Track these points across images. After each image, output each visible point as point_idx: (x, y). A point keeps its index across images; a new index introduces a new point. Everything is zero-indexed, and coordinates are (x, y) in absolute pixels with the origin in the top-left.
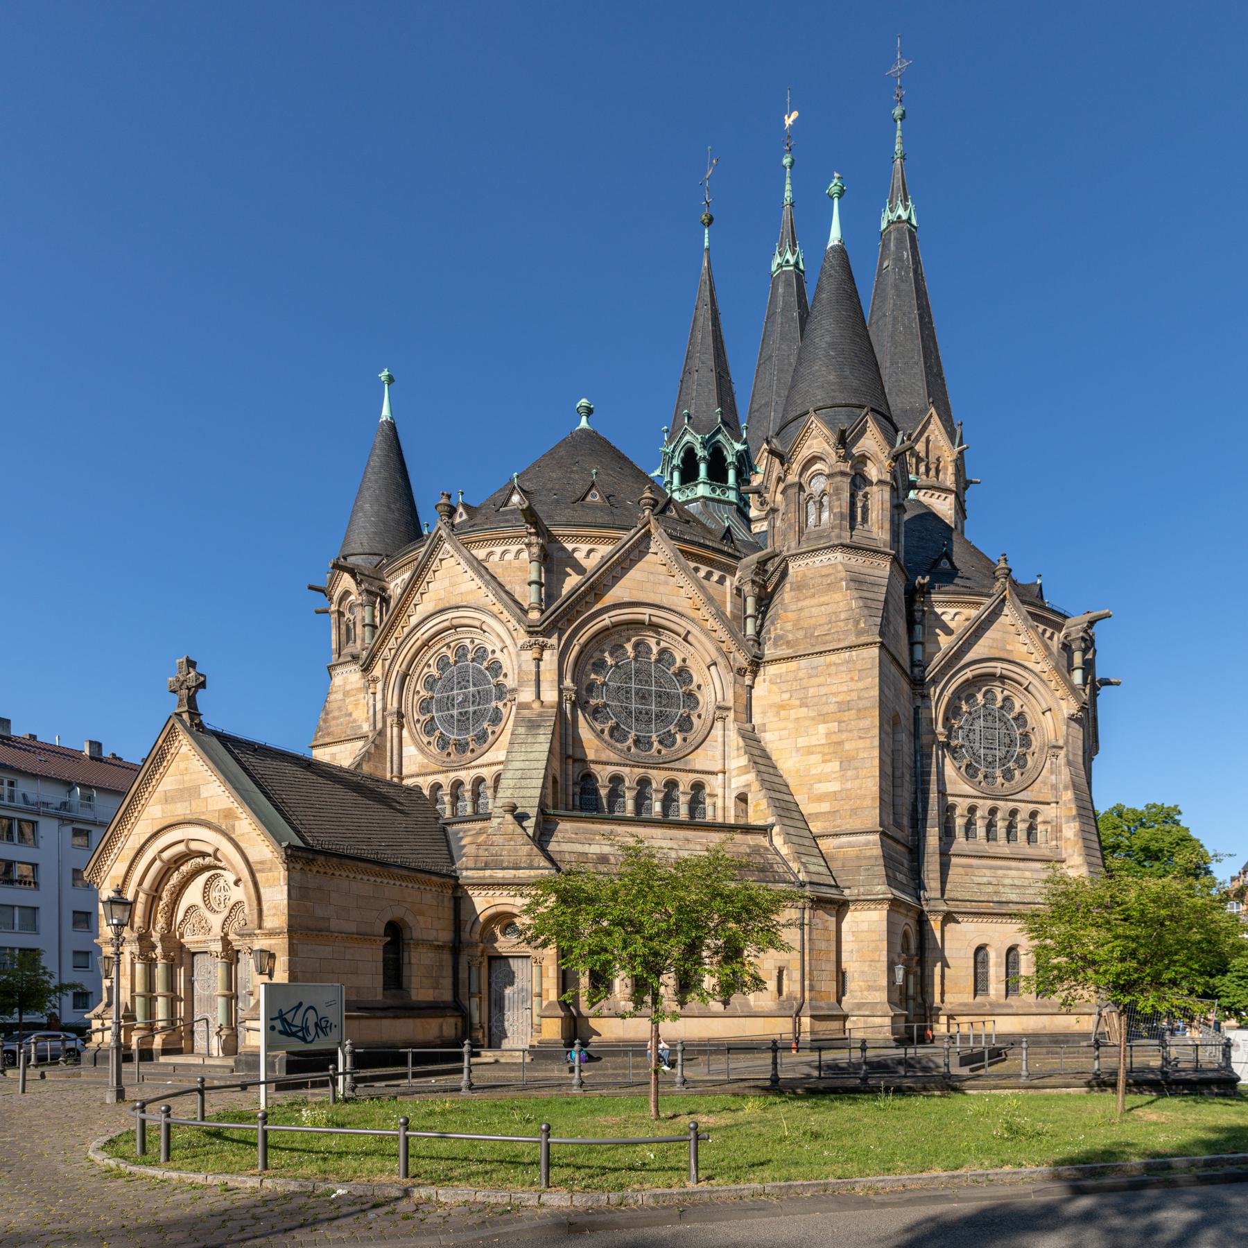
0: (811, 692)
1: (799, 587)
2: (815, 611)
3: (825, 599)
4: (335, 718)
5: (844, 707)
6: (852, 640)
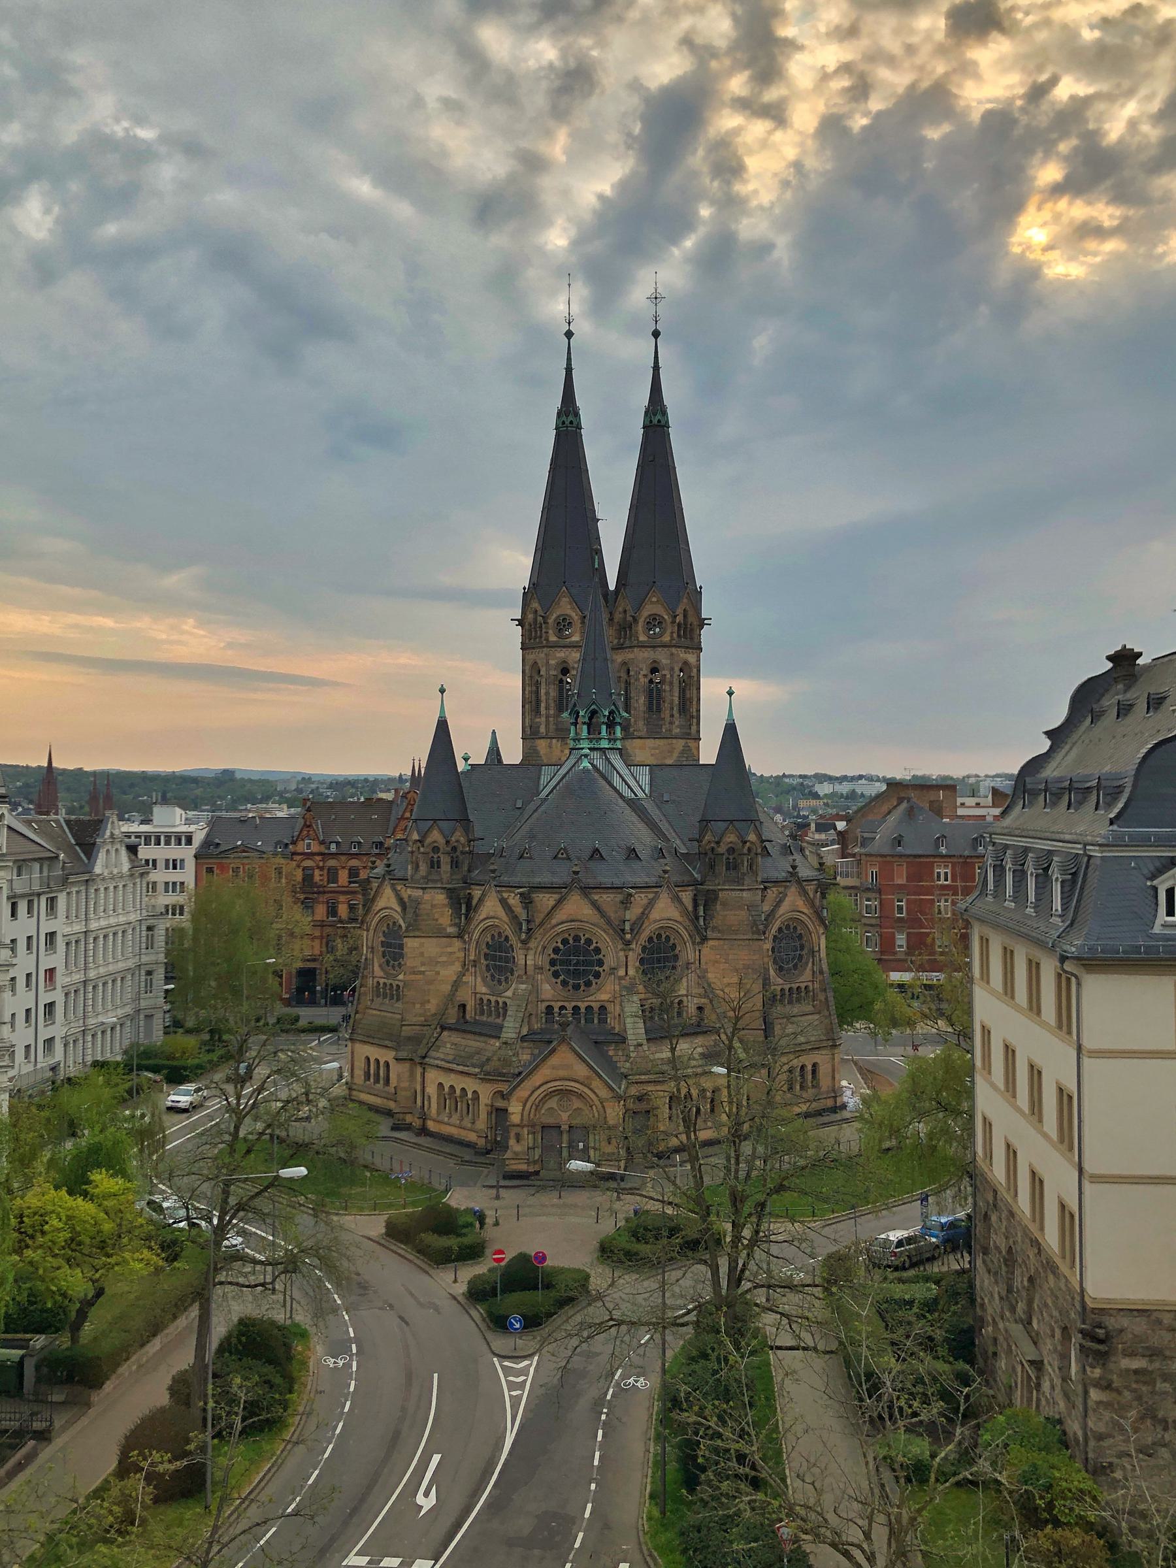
1: (724, 904)
4: (423, 920)
5: (747, 967)
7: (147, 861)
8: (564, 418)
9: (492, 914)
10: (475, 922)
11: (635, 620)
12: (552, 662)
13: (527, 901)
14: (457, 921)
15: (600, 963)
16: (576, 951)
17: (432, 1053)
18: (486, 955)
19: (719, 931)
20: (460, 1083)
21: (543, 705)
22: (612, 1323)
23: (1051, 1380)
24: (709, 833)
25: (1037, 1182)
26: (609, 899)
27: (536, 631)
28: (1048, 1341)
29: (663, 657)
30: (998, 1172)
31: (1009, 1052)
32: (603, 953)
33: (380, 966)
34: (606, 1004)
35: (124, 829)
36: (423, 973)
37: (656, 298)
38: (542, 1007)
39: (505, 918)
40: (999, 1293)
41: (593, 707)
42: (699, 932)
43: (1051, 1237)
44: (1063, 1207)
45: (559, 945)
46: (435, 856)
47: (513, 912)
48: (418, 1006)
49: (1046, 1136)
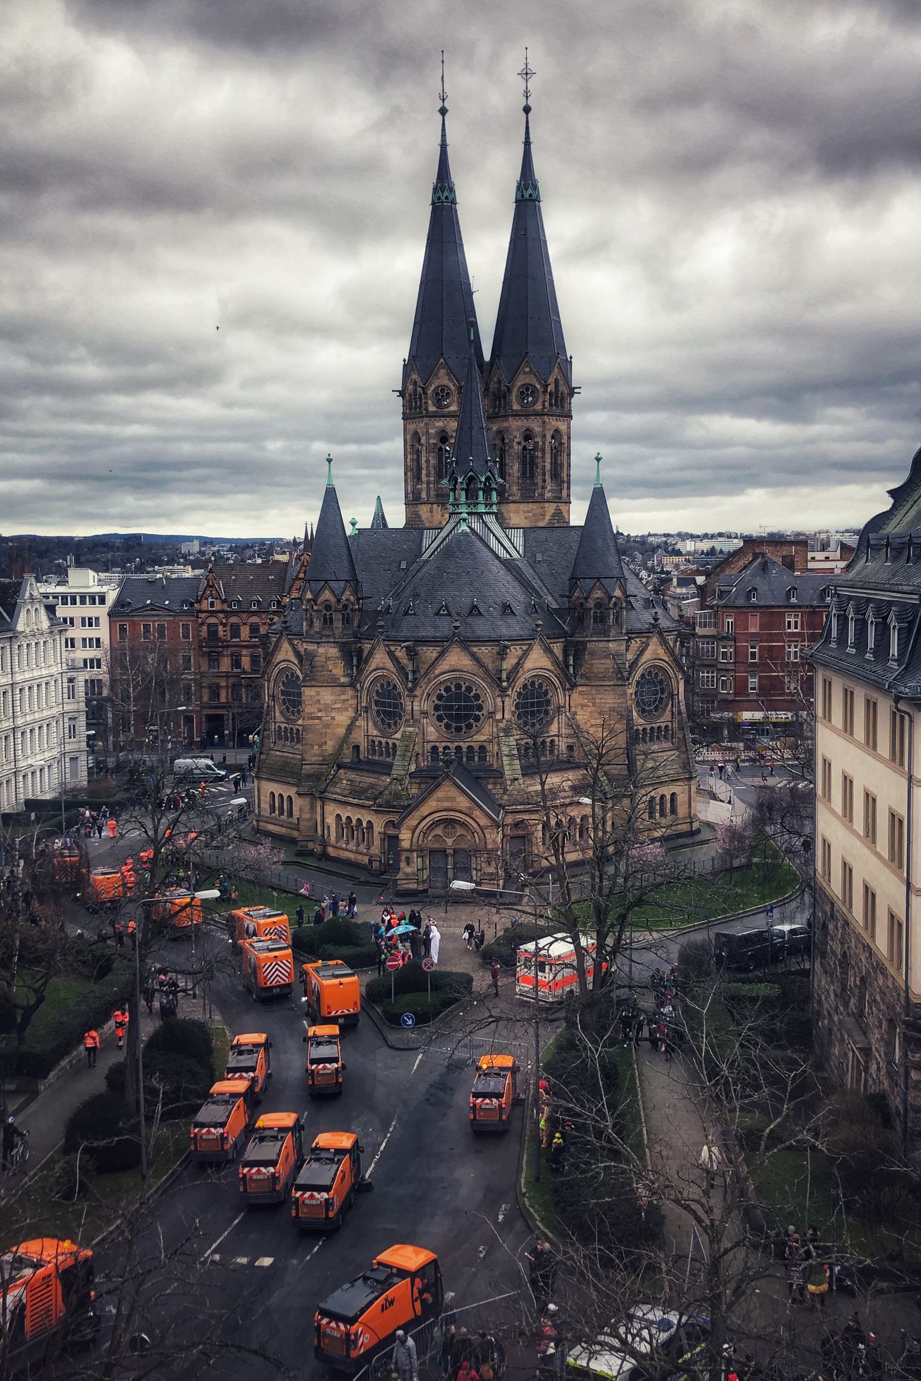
0: (598, 701)
2: (599, 666)
3: (603, 661)
7: (65, 620)
8: (440, 194)
9: (381, 665)
10: (366, 673)
11: (509, 390)
12: (431, 431)
13: (412, 654)
14: (349, 672)
15: (480, 708)
16: (458, 697)
17: (330, 789)
18: (376, 701)
19: (588, 678)
20: (355, 815)
21: (424, 472)
22: (491, 1020)
23: (878, 1063)
24: (578, 590)
25: (870, 896)
27: (416, 402)
28: (876, 1031)
29: (535, 425)
30: (836, 887)
31: (848, 782)
32: (482, 699)
33: (281, 712)
34: (485, 744)
35: (42, 590)
36: (320, 718)
37: (527, 74)
38: (428, 747)
39: (393, 669)
40: (834, 991)
41: (471, 473)
42: (569, 680)
43: (881, 943)
44: (892, 917)
45: (443, 692)
46: (328, 614)
47: (400, 663)
48: (316, 747)
49: (878, 855)
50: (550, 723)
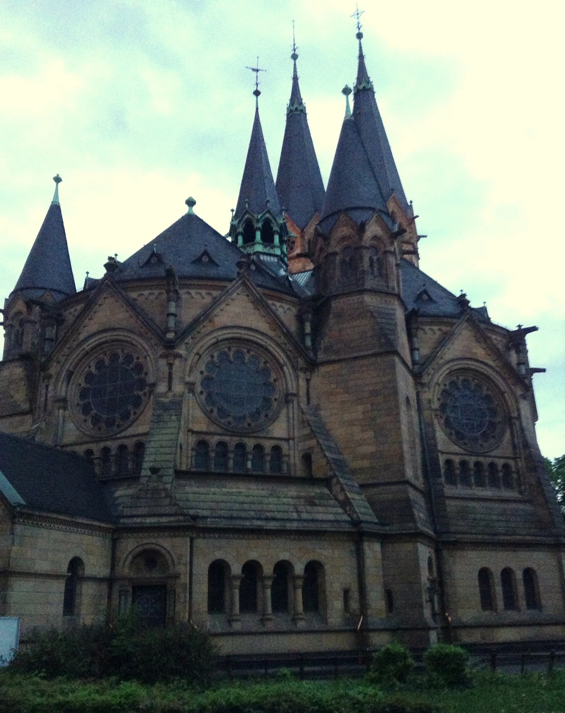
0: (351, 384)
6: (377, 350)
26: (152, 297)
50: (274, 419)
